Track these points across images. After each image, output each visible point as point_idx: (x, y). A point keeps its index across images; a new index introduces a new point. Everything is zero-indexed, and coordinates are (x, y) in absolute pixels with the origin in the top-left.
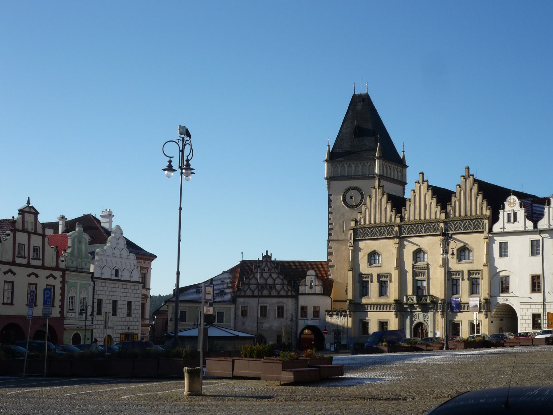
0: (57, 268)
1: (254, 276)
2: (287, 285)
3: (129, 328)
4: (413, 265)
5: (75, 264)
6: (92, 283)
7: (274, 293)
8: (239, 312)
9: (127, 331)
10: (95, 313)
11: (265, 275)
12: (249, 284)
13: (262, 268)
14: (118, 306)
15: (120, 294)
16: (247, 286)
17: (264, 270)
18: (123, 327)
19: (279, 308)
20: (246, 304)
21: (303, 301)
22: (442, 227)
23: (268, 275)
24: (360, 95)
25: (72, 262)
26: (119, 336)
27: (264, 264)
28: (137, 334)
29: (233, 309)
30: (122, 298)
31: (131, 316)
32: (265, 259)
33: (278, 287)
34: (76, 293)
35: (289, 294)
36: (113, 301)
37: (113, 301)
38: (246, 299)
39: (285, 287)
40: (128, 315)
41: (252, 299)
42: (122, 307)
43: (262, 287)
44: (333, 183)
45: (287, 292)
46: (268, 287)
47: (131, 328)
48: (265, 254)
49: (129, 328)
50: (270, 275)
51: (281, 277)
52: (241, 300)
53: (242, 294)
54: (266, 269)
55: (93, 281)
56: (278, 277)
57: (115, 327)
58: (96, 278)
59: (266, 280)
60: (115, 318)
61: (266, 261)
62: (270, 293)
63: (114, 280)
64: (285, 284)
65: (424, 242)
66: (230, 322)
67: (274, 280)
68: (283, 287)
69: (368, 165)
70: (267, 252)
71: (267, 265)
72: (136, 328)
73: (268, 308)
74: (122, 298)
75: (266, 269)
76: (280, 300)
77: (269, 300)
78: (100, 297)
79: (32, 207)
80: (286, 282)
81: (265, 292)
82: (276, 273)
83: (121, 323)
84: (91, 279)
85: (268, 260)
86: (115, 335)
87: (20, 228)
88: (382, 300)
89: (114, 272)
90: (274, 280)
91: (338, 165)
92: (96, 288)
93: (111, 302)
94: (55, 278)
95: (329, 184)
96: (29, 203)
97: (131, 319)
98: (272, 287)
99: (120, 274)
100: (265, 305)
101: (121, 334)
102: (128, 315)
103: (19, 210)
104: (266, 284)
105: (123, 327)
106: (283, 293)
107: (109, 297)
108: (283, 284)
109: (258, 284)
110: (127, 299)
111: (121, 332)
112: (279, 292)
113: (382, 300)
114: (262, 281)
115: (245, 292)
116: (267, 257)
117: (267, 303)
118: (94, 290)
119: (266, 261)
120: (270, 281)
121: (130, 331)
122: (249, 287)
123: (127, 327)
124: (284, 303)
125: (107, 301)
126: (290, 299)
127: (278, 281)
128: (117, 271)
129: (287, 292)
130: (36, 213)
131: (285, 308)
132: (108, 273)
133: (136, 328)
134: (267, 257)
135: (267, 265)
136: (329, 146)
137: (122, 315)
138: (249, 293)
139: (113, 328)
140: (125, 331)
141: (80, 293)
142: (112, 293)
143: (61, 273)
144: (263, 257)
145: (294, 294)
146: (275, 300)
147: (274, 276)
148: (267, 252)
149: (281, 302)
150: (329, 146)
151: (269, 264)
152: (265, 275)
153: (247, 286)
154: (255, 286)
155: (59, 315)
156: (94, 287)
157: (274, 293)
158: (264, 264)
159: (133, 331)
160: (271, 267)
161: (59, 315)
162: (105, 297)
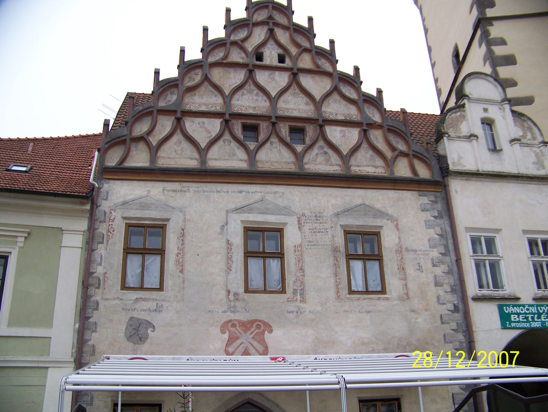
1: (206, 78)
7: (319, 162)
13: (250, 46)
17: (260, 57)
21: (470, 203)
35: (402, 169)
38: (155, 191)
41: (193, 187)
45: (389, 164)
46: (284, 129)
53: (139, 158)
56: (335, 89)
62: (299, 157)
64: (372, 125)
66: (48, 322)
71: (271, 33)
77: (297, 197)
85: (280, 18)
100: (272, 219)
106: (366, 164)
109: (227, 118)
114: (248, 103)
115: (154, 151)
117: (287, 211)
124: (381, 214)
149: (366, 209)
160: (294, 51)
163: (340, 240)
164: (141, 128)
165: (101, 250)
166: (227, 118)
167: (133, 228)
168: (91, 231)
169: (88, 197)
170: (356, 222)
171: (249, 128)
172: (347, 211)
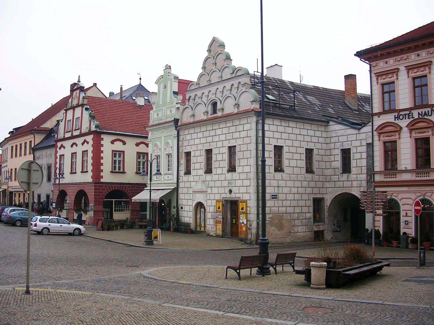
3: (231, 191)
9: (228, 195)
10: (182, 173)
15: (216, 139)
18: (222, 190)
26: (214, 203)
28: (245, 201)
30: (220, 144)
31: (282, 171)
40: (229, 171)
42: (220, 157)
47: (234, 190)
49: (231, 191)
57: (209, 191)
60: (278, 175)
72: (243, 190)
74: (220, 144)
78: (188, 149)
83: (218, 184)
86: (209, 203)
92: (181, 138)
94: (88, 143)
97: (235, 175)
99: (219, 106)
101: (217, 201)
102: (229, 171)
105: (222, 190)
107: (200, 147)
110: (227, 144)
111: (218, 197)
121: (233, 195)
125: (198, 153)
133: (243, 190)
137: (219, 171)
140: (224, 196)
142: (203, 141)
159: (237, 195)
162: (194, 148)
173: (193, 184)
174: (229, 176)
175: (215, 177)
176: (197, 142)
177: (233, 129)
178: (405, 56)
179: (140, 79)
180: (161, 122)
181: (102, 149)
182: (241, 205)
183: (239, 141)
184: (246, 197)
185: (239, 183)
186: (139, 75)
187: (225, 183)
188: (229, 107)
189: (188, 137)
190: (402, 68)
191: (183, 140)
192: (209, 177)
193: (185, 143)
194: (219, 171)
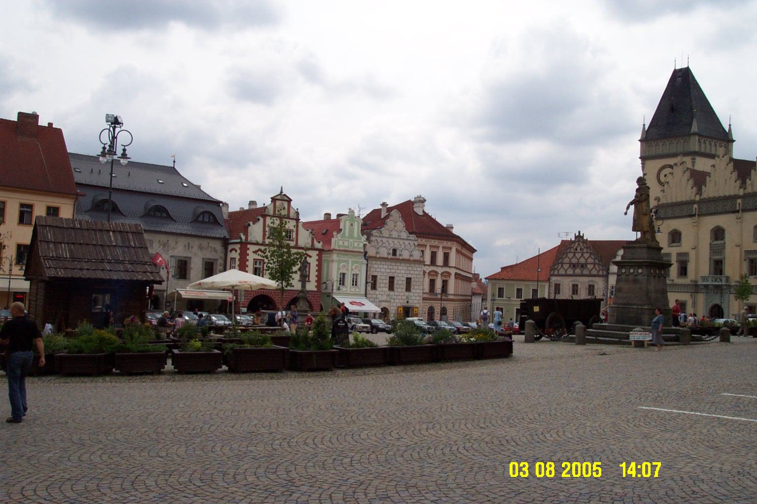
0: (313, 248)
2: (599, 265)
3: (408, 302)
4: (710, 244)
5: (346, 244)
6: (365, 262)
7: (585, 272)
8: (553, 289)
9: (406, 304)
11: (577, 255)
12: (562, 264)
13: (575, 248)
14: (396, 282)
16: (560, 266)
17: (576, 249)
18: (402, 301)
19: (590, 286)
20: (558, 282)
22: (739, 204)
23: (580, 254)
24: (681, 70)
25: (343, 243)
27: (577, 244)
29: (547, 287)
32: (577, 240)
33: (590, 267)
34: (347, 270)
35: (601, 273)
36: (390, 277)
37: (390, 277)
38: (558, 278)
39: (597, 266)
42: (400, 282)
43: (574, 266)
44: (648, 163)
46: (580, 266)
47: (410, 301)
48: (577, 234)
49: (408, 302)
50: (582, 254)
51: (593, 257)
52: (553, 279)
53: (556, 272)
54: (579, 249)
55: (365, 259)
56: (590, 256)
57: (392, 301)
58: (371, 257)
59: (578, 260)
61: (579, 241)
62: (582, 271)
63: (391, 259)
65: (722, 220)
67: (586, 260)
68: (594, 266)
69: (682, 141)
70: (579, 232)
71: (579, 244)
72: (415, 301)
73: (579, 286)
75: (579, 249)
76: (591, 278)
78: (375, 274)
79: (285, 195)
80: (597, 262)
81: (578, 271)
82: (587, 252)
84: (363, 258)
85: (581, 240)
87: (271, 213)
88: (682, 281)
89: (391, 252)
90: (586, 260)
91: (653, 144)
92: (369, 265)
93: (388, 278)
95: (643, 164)
96: (281, 192)
98: (583, 266)
99: (398, 253)
100: (576, 283)
101: (398, 307)
103: (272, 198)
104: (578, 264)
108: (595, 264)
109: (570, 264)
110: (406, 276)
111: (399, 305)
112: (590, 271)
113: (682, 281)
114: (574, 261)
115: (558, 271)
116: (579, 237)
118: (367, 267)
119: (579, 241)
120: (582, 261)
121: (409, 304)
122: (562, 266)
123: (406, 301)
124: (596, 282)
126: (601, 278)
127: (590, 260)
128: (395, 251)
129: (598, 272)
130: (289, 201)
131: (596, 287)
132: (384, 252)
134: (579, 237)
135: (579, 244)
136: (644, 125)
138: (562, 272)
139: (390, 301)
141: (352, 270)
143: (317, 252)
144: (576, 237)
145: (605, 273)
146: (586, 279)
147: (586, 255)
148: (579, 232)
149: (592, 281)
150: (644, 125)
151: (581, 243)
152: (578, 255)
153: (560, 266)
154: (568, 265)
155: (315, 289)
156: (367, 265)
157: (585, 272)
158: (577, 244)
160: (583, 247)
161: (315, 289)
163: (587, 286)
164: (556, 266)
165: (551, 288)
166: (570, 264)
167: (556, 285)
168: (549, 285)
169: (549, 280)
170: (591, 283)
171: (574, 266)
172: (589, 281)
173: (379, 296)
174: (407, 294)
175: (396, 293)
176: (382, 270)
177: (410, 268)
178: (430, 240)
179: (174, 162)
180: (348, 249)
181: (317, 263)
182: (415, 310)
183: (415, 276)
184: (417, 305)
185: (414, 298)
186: (173, 158)
187: (405, 298)
188: (406, 255)
189: (376, 266)
190: (428, 245)
191: (371, 267)
192: (392, 293)
193: (372, 270)
194: (400, 290)
